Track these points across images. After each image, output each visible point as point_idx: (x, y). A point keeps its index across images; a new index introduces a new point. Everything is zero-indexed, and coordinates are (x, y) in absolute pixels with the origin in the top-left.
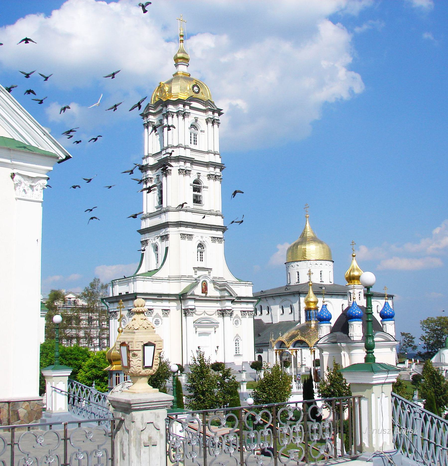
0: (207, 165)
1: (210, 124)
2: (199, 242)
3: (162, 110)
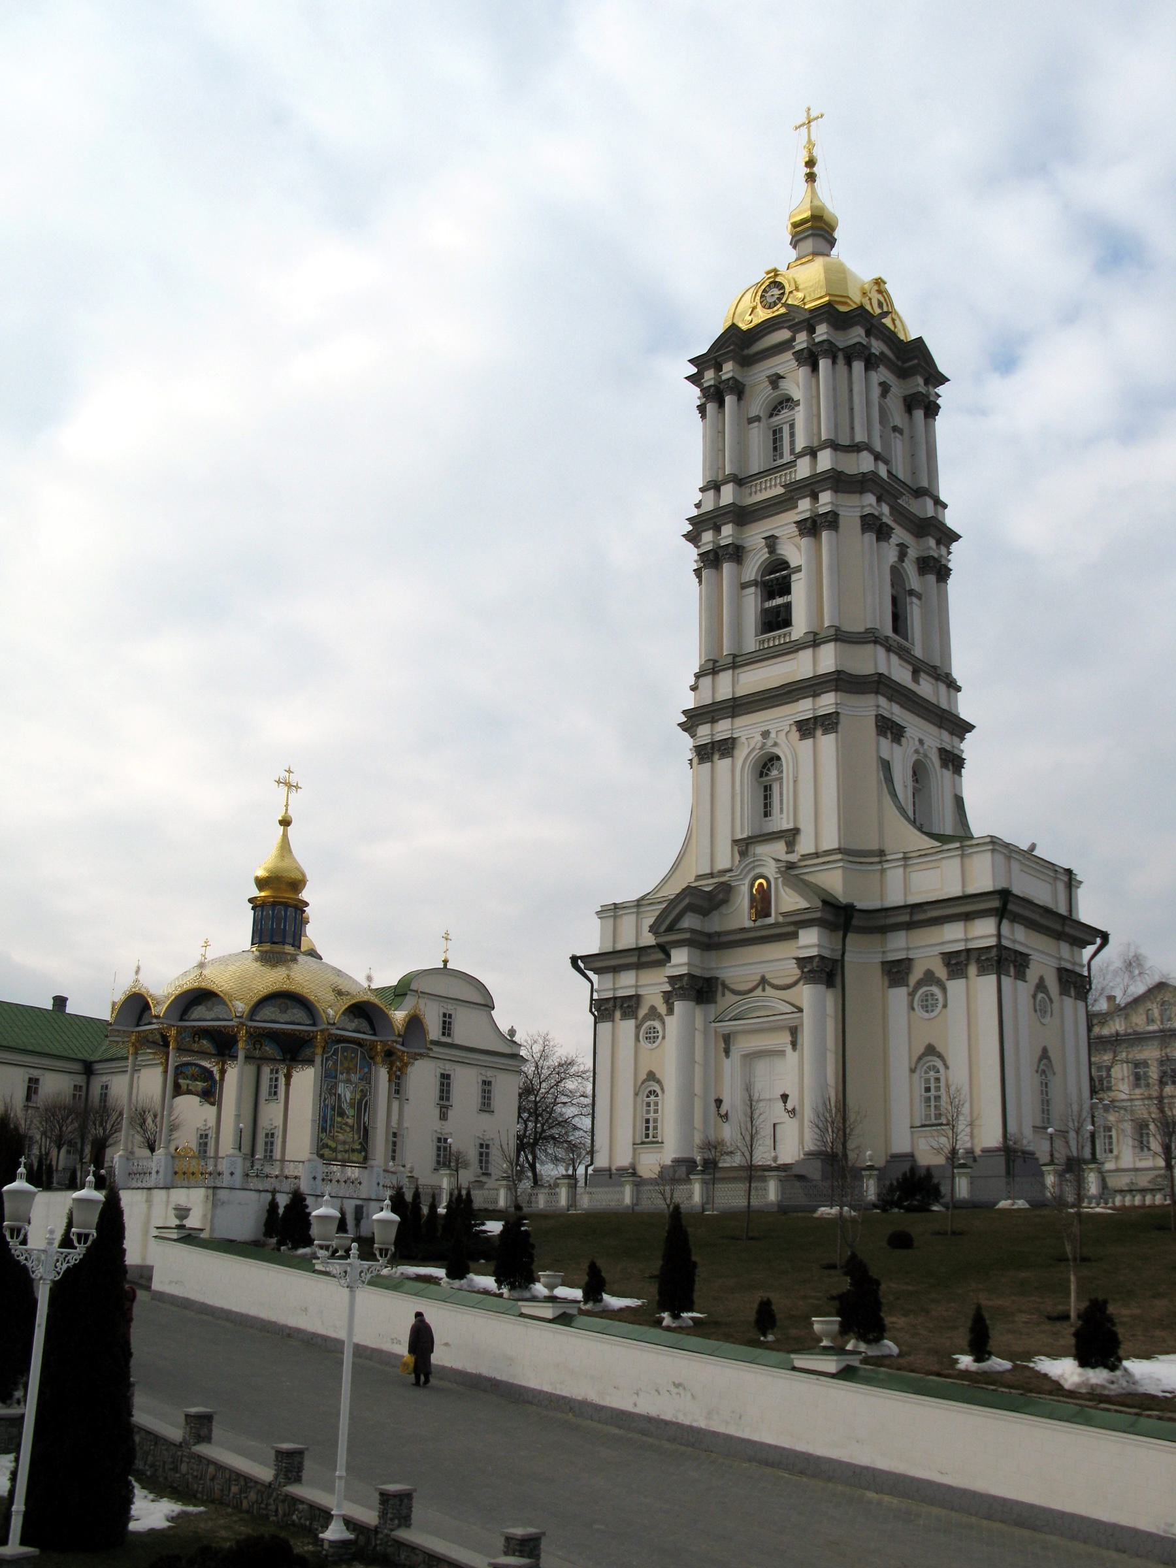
1: (919, 414)
3: (793, 339)
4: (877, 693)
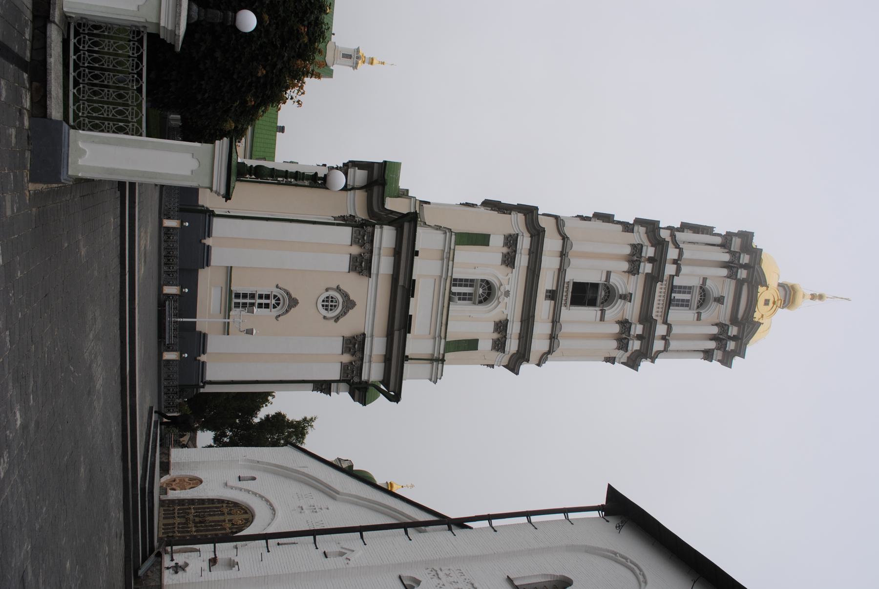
0: (646, 319)
1: (715, 330)
4: (531, 237)
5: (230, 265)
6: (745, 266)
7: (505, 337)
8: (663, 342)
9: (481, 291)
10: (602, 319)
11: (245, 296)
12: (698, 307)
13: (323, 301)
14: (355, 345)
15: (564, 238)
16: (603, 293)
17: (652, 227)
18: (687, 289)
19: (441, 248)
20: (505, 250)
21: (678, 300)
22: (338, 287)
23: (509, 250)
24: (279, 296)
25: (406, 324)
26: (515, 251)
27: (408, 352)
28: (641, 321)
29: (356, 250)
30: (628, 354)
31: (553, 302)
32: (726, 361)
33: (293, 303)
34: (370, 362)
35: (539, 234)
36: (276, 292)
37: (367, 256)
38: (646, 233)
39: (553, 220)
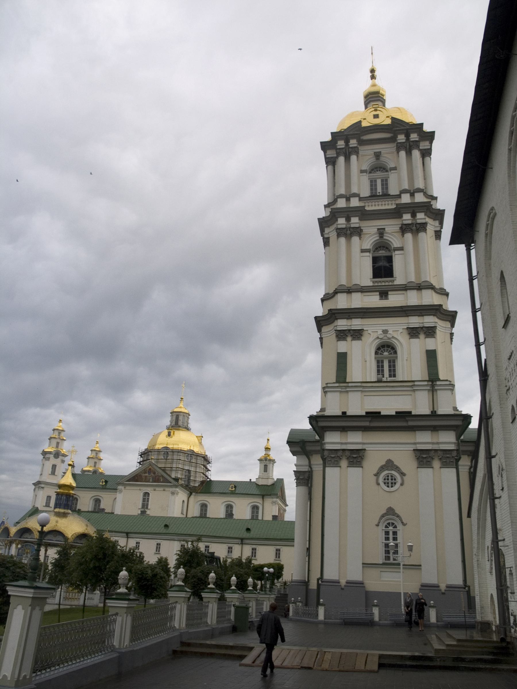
0: (397, 213)
1: (403, 154)
2: (377, 342)
4: (337, 319)
5: (361, 565)
6: (347, 142)
7: (422, 328)
8: (416, 194)
9: (386, 353)
10: (401, 249)
11: (387, 552)
12: (387, 171)
13: (388, 487)
14: (424, 458)
15: (336, 292)
16: (380, 252)
17: (323, 223)
18: (373, 184)
19: (338, 394)
20: (349, 339)
21: (382, 189)
22: (375, 475)
23: (349, 335)
24: (386, 524)
25: (403, 415)
26: (349, 330)
27: (427, 411)
28: (402, 217)
29: (344, 463)
30: (428, 220)
31: (389, 293)
32: (431, 136)
33: (390, 511)
34: (438, 443)
35: (334, 314)
36: (382, 527)
37: (348, 453)
38: (329, 227)
39: (325, 303)
